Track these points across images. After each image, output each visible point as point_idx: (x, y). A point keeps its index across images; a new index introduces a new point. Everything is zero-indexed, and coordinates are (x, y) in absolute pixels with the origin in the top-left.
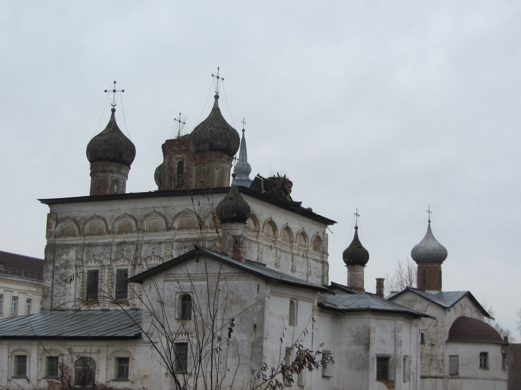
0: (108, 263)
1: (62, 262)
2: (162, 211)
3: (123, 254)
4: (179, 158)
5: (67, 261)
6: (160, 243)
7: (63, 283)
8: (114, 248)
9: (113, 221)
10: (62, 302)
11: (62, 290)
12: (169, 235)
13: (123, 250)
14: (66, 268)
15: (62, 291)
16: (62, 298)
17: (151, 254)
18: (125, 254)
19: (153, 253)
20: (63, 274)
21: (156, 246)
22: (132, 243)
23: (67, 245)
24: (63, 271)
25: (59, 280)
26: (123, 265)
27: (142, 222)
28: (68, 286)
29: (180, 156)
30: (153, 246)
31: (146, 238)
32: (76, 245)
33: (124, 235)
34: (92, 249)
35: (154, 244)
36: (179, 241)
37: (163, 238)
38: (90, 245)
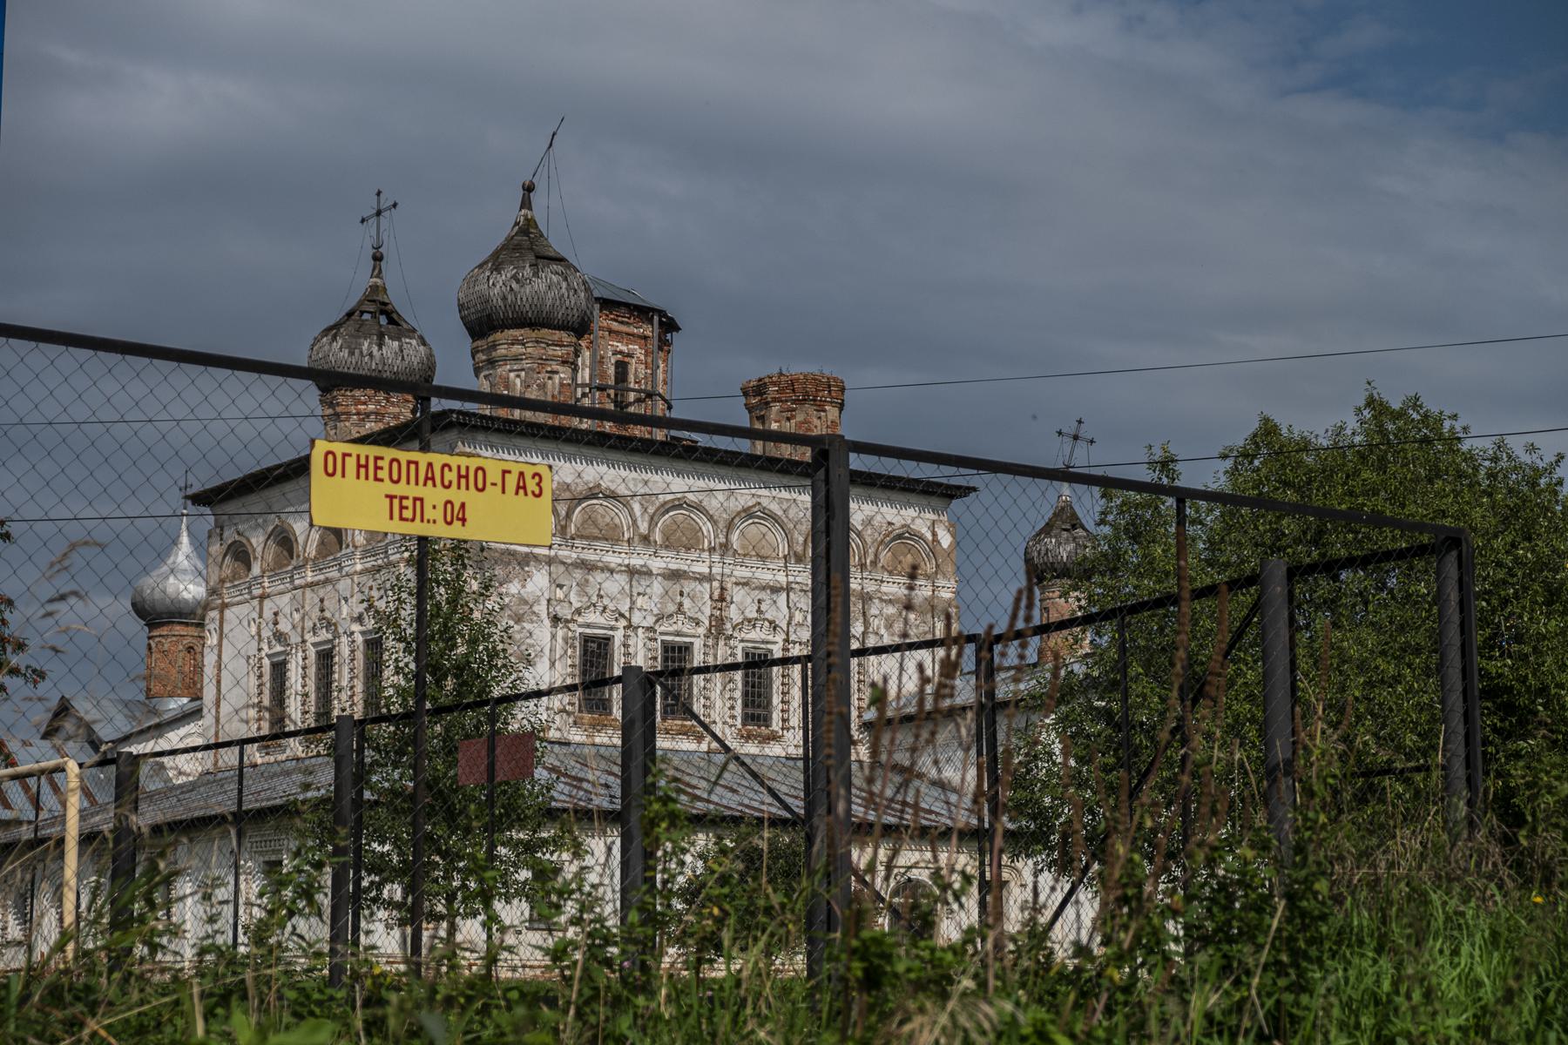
0: (650, 621)
2: (775, 507)
3: (681, 604)
4: (621, 352)
6: (775, 590)
8: (657, 587)
9: (651, 510)
13: (682, 594)
17: (755, 615)
18: (687, 603)
19: (759, 611)
22: (709, 578)
26: (678, 634)
27: (730, 526)
29: (625, 349)
31: (742, 573)
32: (550, 561)
34: (599, 576)
35: (763, 588)
38: (588, 567)
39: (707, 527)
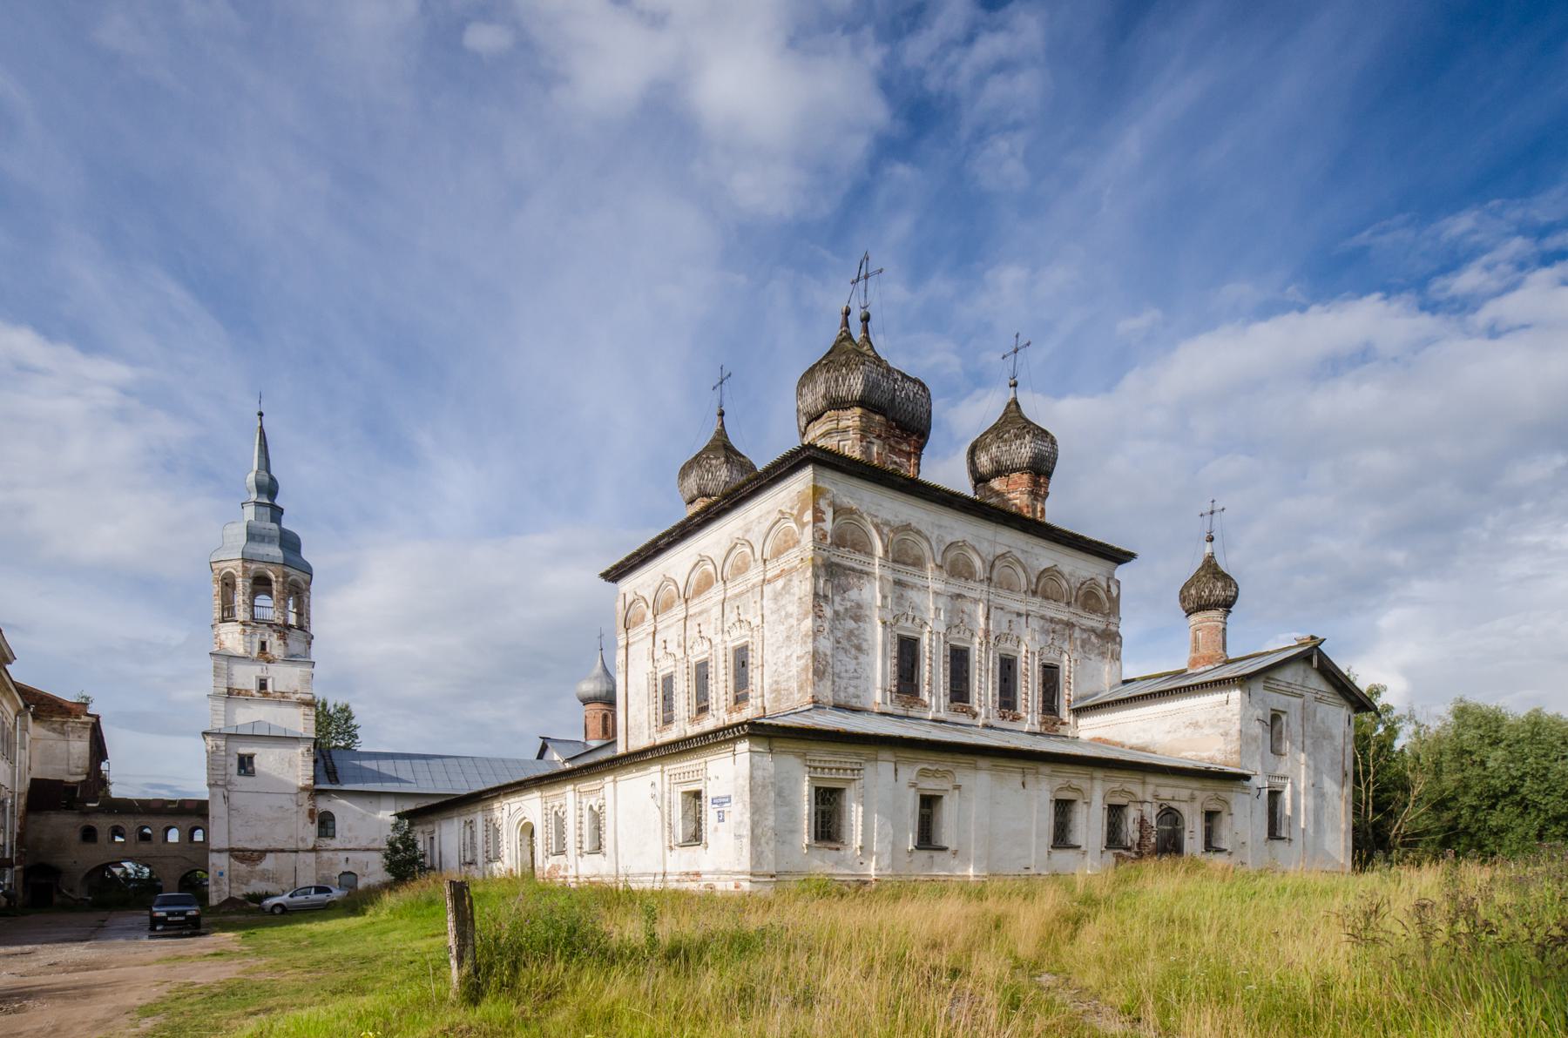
1: (849, 604)
5: (859, 606)
6: (1019, 615)
7: (853, 651)
10: (851, 690)
11: (852, 665)
12: (1035, 605)
14: (857, 618)
15: (851, 667)
16: (853, 682)
20: (851, 632)
21: (1014, 617)
23: (853, 570)
24: (851, 624)
25: (844, 643)
28: (862, 658)
30: (1009, 617)
33: (962, 582)
36: (1042, 617)
37: (1022, 608)
39: (978, 563)
